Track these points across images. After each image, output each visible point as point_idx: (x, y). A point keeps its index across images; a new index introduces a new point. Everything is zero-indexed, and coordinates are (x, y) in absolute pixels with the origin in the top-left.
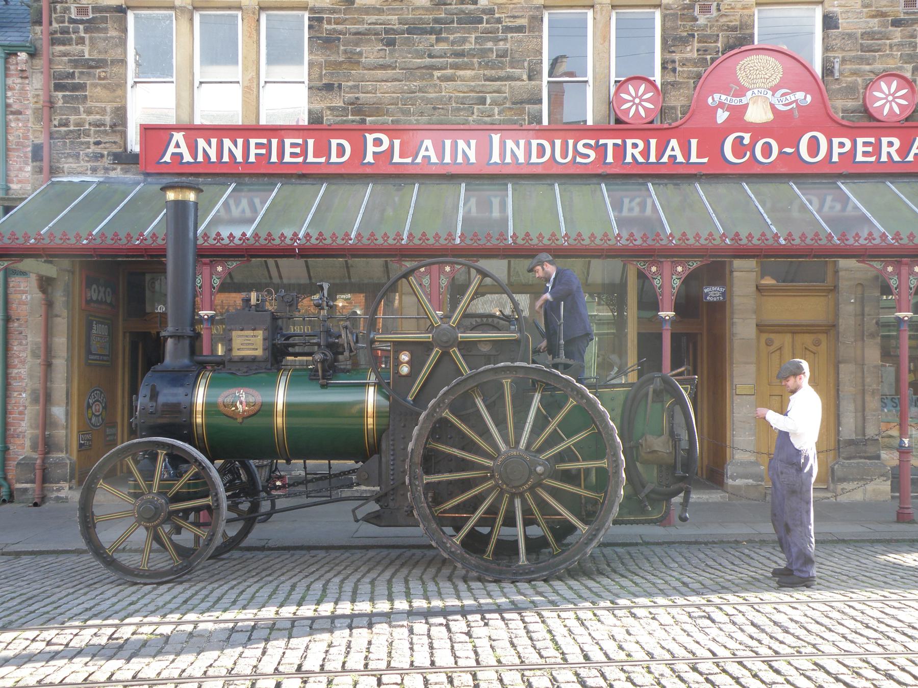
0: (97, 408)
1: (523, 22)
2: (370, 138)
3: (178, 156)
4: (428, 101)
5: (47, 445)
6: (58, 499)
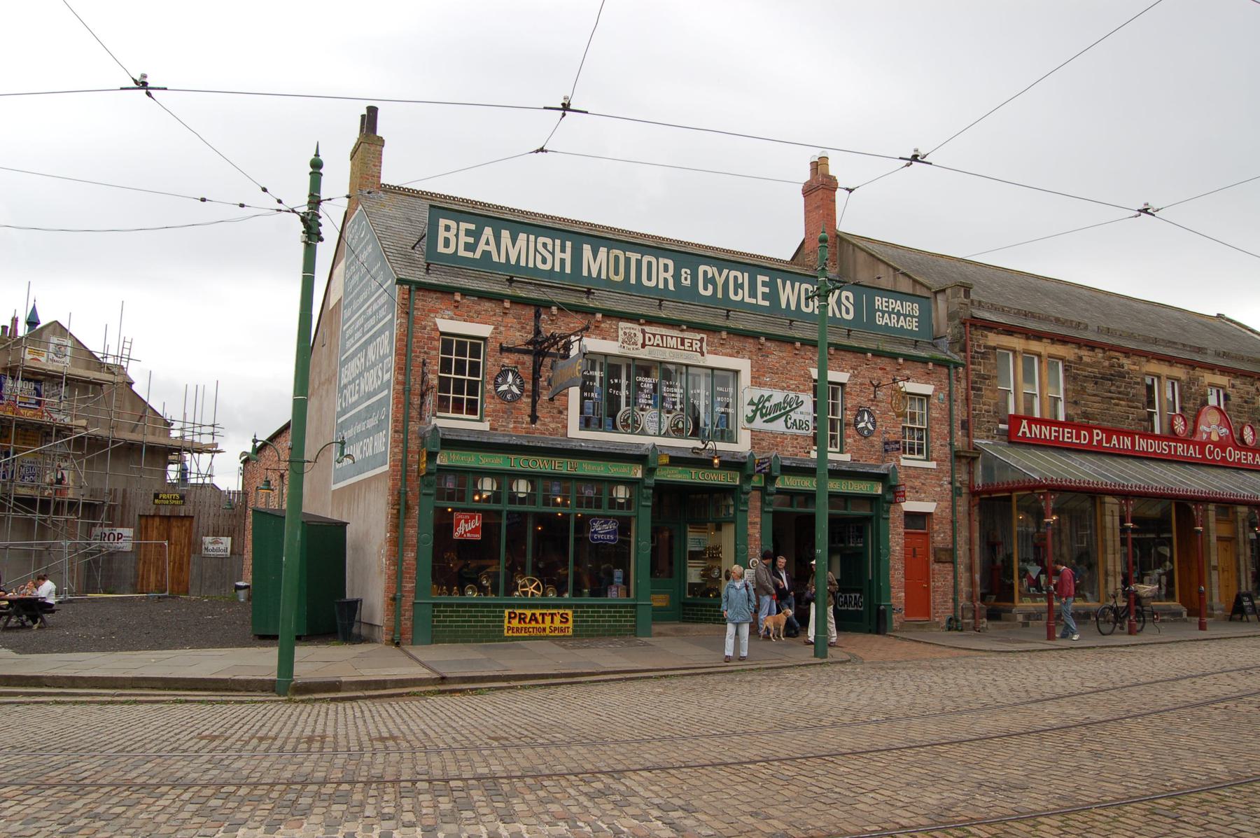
2: (1095, 431)
3: (1024, 433)
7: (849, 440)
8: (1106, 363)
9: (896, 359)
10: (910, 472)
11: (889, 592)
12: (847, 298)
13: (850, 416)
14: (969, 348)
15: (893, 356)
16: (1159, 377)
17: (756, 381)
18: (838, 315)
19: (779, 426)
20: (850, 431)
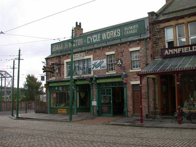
0: (164, 101)
5: (155, 108)
6: (157, 118)
17: (94, 59)
19: (99, 68)
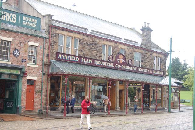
1: (101, 46)
4: (91, 55)
7: (11, 58)
8: (92, 40)
9: (28, 35)
10: (30, 68)
11: (21, 102)
12: (14, 16)
13: (12, 51)
14: (50, 33)
15: (27, 34)
16: (106, 45)
18: (11, 21)
20: (12, 55)
